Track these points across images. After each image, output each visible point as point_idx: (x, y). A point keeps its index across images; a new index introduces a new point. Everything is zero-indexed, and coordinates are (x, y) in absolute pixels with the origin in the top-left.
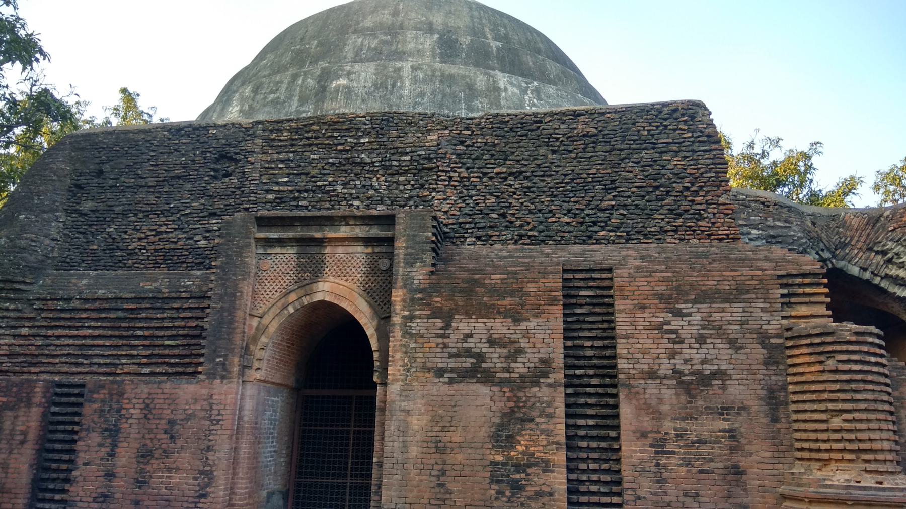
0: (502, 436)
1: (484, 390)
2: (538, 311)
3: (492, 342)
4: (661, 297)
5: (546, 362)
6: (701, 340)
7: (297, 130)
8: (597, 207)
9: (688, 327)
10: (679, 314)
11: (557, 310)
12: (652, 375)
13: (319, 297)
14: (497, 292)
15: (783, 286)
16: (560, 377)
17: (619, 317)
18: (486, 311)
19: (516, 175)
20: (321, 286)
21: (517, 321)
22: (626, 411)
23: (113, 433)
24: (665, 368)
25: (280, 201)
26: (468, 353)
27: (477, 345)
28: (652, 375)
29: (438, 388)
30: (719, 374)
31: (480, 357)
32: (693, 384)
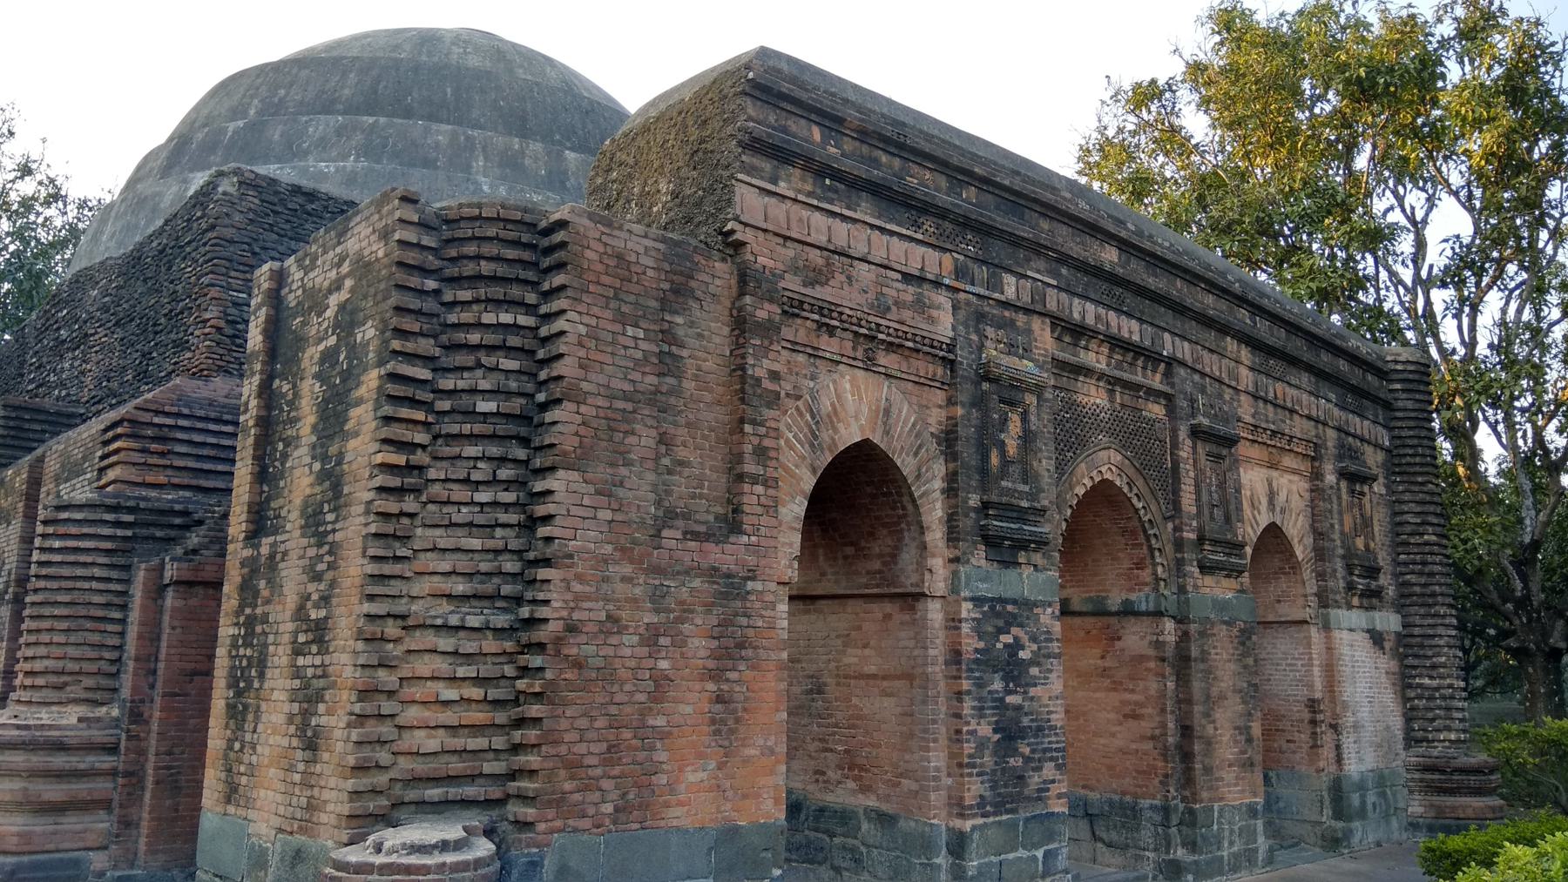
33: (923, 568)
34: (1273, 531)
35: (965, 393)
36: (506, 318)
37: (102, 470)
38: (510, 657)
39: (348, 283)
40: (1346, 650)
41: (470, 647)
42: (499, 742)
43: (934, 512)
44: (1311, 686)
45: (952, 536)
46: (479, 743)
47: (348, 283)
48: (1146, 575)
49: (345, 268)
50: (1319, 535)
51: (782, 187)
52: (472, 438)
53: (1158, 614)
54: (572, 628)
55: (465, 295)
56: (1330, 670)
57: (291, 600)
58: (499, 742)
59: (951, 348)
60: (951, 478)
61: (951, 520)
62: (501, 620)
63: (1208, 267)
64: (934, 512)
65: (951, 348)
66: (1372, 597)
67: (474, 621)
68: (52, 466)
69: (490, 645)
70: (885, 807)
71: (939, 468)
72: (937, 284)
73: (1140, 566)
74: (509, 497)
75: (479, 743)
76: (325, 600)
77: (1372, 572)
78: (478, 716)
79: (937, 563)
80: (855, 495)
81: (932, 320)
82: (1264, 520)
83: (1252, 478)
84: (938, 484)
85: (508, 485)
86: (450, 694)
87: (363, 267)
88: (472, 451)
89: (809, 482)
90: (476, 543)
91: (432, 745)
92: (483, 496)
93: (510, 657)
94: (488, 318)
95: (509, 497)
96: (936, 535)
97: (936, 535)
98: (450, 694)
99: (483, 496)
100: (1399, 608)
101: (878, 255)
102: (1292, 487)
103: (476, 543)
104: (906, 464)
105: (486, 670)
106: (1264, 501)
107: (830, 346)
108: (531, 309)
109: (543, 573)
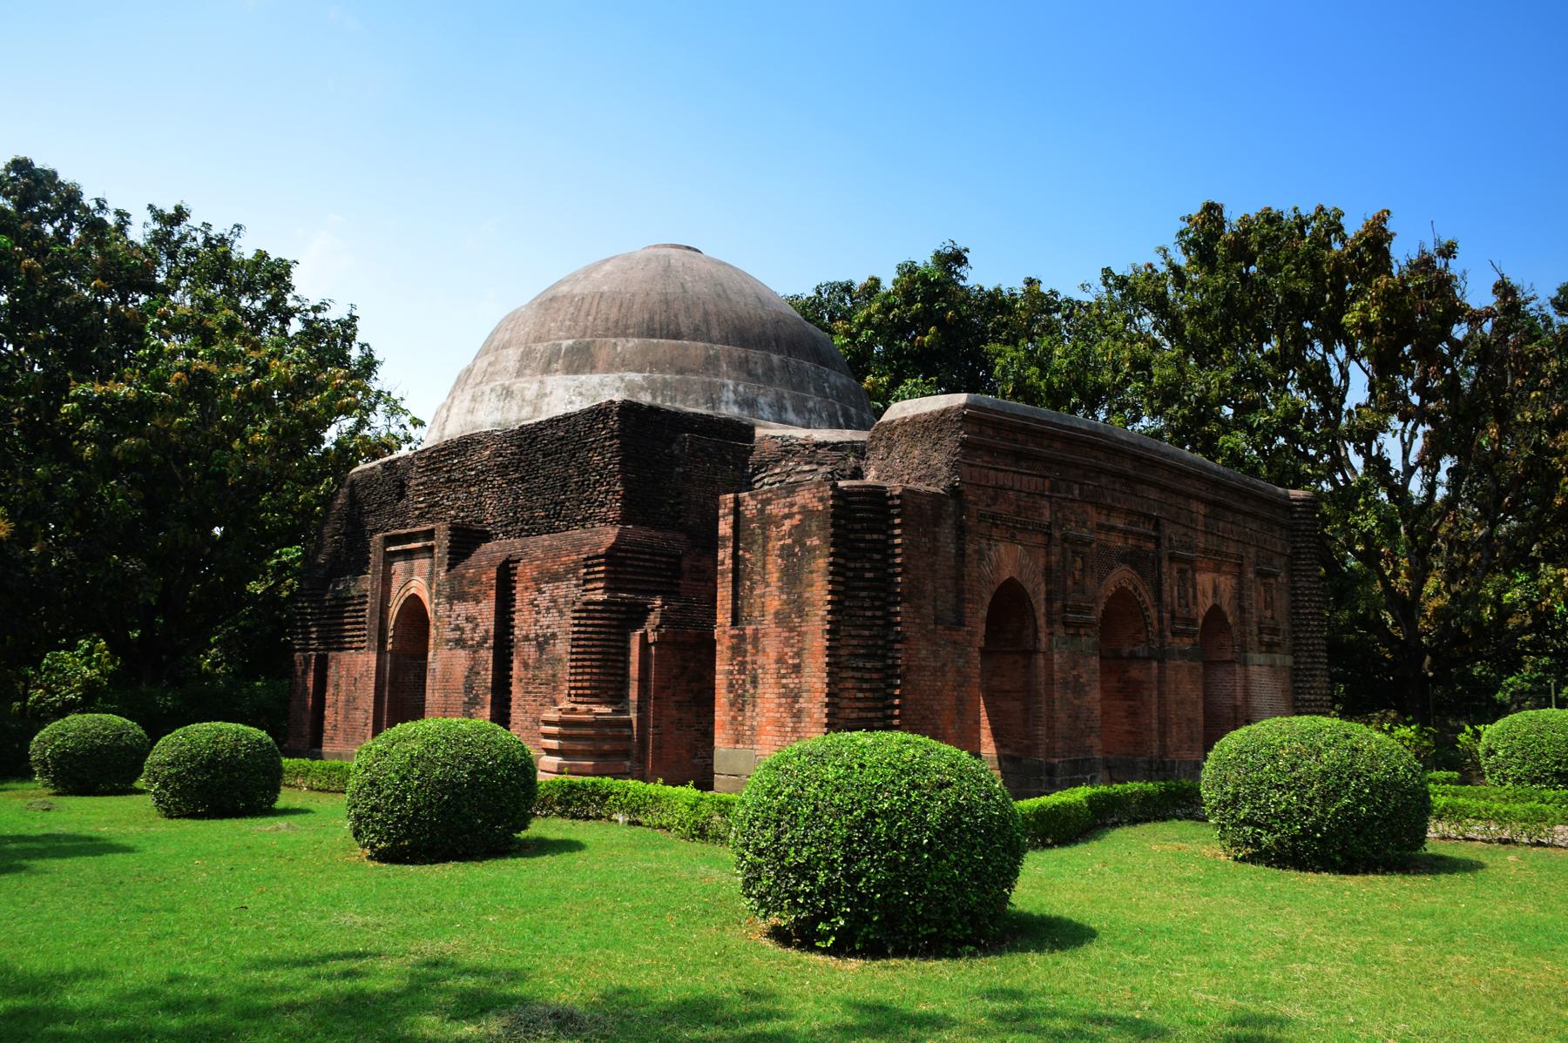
0: (469, 688)
1: (462, 653)
2: (487, 596)
3: (467, 619)
4: (534, 580)
5: (487, 631)
6: (548, 609)
7: (429, 458)
8: (556, 504)
9: (544, 601)
10: (540, 592)
11: (493, 593)
12: (526, 638)
13: (413, 591)
14: (473, 582)
15: (586, 566)
16: (491, 642)
17: (518, 597)
18: (462, 597)
19: (522, 479)
20: (413, 583)
21: (478, 602)
22: (516, 665)
23: (337, 686)
24: (532, 636)
25: (421, 516)
26: (457, 628)
27: (461, 622)
28: (526, 638)
29: (444, 652)
30: (554, 635)
31: (462, 630)
32: (543, 643)
33: (1036, 638)
34: (1215, 611)
35: (1056, 550)
36: (875, 536)
37: (586, 581)
38: (882, 680)
39: (798, 517)
40: (1254, 677)
41: (867, 676)
42: (880, 714)
43: (1041, 611)
44: (1235, 698)
45: (1050, 622)
46: (871, 715)
47: (798, 517)
48: (1142, 637)
49: (795, 509)
50: (1242, 609)
51: (978, 461)
52: (863, 589)
53: (1148, 659)
54: (909, 668)
55: (858, 526)
56: (1246, 689)
57: (773, 655)
58: (880, 714)
59: (1049, 527)
60: (1049, 593)
61: (1048, 614)
62: (879, 665)
63: (1181, 460)
64: (1041, 611)
65: (1049, 527)
66: (1270, 647)
67: (868, 665)
68: (525, 571)
69: (875, 676)
70: (1016, 754)
71: (1043, 587)
72: (1042, 495)
73: (1139, 632)
74: (879, 613)
75: (871, 715)
76: (798, 654)
77: (1274, 631)
78: (871, 704)
79: (1042, 636)
80: (1009, 602)
81: (1041, 515)
82: (1210, 603)
83: (1205, 580)
84: (1043, 596)
85: (878, 608)
86: (860, 695)
87: (807, 512)
88: (863, 594)
89: (988, 599)
90: (867, 633)
91: (854, 715)
92: (869, 614)
93: (882, 680)
94: (868, 537)
95: (879, 613)
96: (1042, 621)
97: (1042, 621)
98: (860, 695)
99: (869, 614)
100: (1293, 652)
101: (1017, 486)
102: (1227, 583)
103: (867, 633)
104: (1029, 587)
105: (874, 685)
106: (1210, 592)
107: (996, 533)
108: (884, 532)
109: (898, 646)
